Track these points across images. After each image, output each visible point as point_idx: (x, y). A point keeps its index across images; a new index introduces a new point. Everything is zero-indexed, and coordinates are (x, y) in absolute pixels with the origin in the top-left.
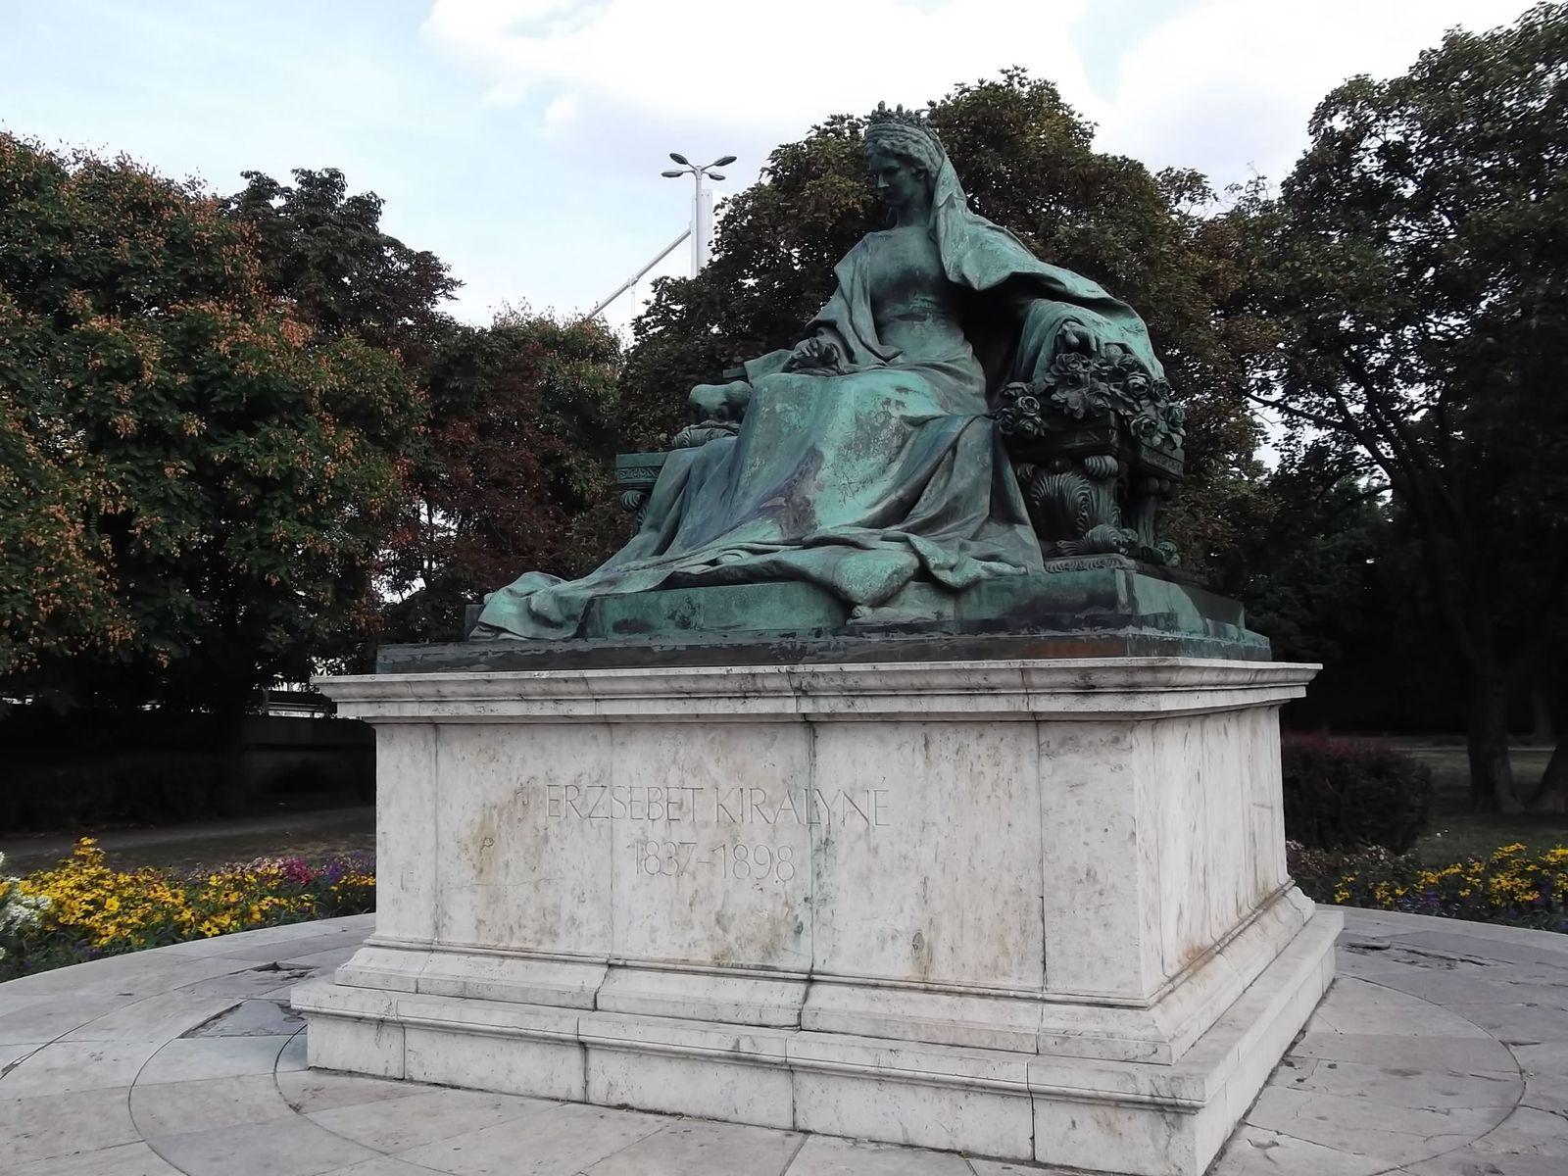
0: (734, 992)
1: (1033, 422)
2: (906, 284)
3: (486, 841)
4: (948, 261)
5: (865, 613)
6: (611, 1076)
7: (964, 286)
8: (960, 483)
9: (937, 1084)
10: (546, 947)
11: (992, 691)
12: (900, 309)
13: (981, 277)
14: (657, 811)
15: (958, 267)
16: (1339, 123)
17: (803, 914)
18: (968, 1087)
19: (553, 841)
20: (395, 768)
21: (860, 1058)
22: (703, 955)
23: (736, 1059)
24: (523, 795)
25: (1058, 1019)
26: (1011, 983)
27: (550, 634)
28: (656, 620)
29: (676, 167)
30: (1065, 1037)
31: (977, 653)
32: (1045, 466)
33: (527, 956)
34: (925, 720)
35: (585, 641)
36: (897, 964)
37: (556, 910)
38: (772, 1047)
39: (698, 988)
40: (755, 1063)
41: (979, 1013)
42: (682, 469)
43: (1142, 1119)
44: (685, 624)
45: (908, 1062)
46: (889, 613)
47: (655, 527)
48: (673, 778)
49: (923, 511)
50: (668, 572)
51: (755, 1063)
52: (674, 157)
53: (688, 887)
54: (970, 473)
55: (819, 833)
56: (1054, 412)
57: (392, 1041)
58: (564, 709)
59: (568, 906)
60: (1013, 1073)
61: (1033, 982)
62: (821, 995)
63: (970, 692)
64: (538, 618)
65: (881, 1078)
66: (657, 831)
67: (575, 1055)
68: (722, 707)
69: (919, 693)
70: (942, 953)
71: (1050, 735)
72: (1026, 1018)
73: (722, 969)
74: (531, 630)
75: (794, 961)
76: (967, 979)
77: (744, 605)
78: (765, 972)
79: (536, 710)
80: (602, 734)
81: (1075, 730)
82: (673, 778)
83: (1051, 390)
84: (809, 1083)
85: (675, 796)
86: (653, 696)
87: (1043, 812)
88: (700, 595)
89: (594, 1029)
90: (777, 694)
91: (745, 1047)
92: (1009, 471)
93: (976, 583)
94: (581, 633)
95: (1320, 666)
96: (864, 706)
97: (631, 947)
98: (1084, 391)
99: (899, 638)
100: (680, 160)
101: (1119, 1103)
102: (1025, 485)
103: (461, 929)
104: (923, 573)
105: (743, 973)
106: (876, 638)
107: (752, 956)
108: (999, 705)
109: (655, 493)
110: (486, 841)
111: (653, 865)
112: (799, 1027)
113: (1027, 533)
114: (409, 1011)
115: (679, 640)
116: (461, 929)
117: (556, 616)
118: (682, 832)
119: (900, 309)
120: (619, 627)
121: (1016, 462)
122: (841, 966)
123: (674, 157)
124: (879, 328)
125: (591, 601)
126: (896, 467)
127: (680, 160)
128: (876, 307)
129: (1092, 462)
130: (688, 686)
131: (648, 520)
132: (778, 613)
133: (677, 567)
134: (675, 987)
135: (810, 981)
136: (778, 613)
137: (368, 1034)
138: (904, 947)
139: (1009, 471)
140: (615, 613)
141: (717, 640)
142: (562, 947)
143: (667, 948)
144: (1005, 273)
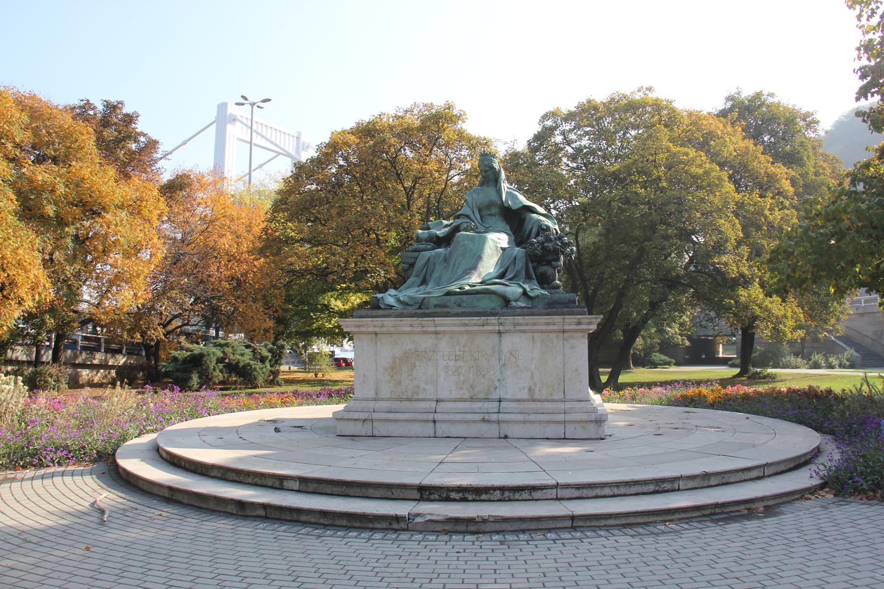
0: (477, 405)
1: (539, 252)
2: (491, 205)
6: (442, 429)
9: (540, 422)
10: (415, 397)
11: (554, 324)
12: (488, 212)
14: (452, 357)
16: (549, 123)
17: (497, 384)
18: (548, 422)
19: (417, 367)
21: (520, 417)
22: (467, 396)
23: (484, 420)
25: (568, 405)
26: (555, 397)
28: (448, 304)
29: (243, 101)
30: (572, 408)
31: (547, 314)
33: (409, 400)
34: (533, 332)
35: (421, 309)
36: (524, 395)
37: (418, 387)
38: (494, 417)
39: (467, 405)
40: (489, 421)
41: (548, 405)
42: (427, 258)
43: (592, 425)
44: (459, 305)
45: (533, 417)
47: (417, 276)
48: (457, 349)
49: (509, 275)
51: (489, 421)
52: (242, 97)
53: (462, 378)
54: (520, 265)
55: (502, 362)
56: (544, 248)
57: (368, 426)
58: (425, 329)
59: (422, 385)
60: (561, 417)
61: (561, 396)
62: (503, 404)
63: (548, 324)
65: (524, 422)
66: (452, 363)
67: (432, 424)
68: (476, 328)
69: (534, 324)
70: (537, 392)
71: (566, 335)
72: (561, 406)
73: (472, 399)
75: (496, 396)
76: (544, 397)
77: (478, 300)
78: (487, 400)
79: (415, 329)
80: (434, 336)
81: (573, 334)
82: (457, 349)
83: (543, 243)
84: (503, 426)
85: (458, 353)
86: (455, 325)
87: (564, 355)
88: (465, 297)
89: (438, 417)
90: (494, 324)
91: (487, 417)
92: (530, 265)
93: (538, 296)
94: (420, 308)
96: (518, 328)
97: (444, 395)
99: (525, 310)
100: (246, 99)
101: (587, 422)
102: (534, 269)
103: (385, 392)
104: (525, 293)
105: (480, 400)
107: (482, 396)
108: (556, 327)
109: (416, 265)
111: (450, 373)
112: (499, 413)
113: (535, 282)
114: (375, 416)
115: (460, 310)
118: (459, 363)
119: (488, 212)
120: (435, 306)
121: (532, 262)
122: (508, 396)
123: (242, 97)
125: (424, 298)
127: (246, 99)
128: (480, 210)
130: (467, 322)
131: (414, 273)
134: (460, 405)
135: (500, 401)
136: (486, 303)
137: (360, 424)
138: (526, 390)
139: (530, 265)
140: (434, 302)
141: (471, 310)
142: (421, 396)
143: (455, 395)
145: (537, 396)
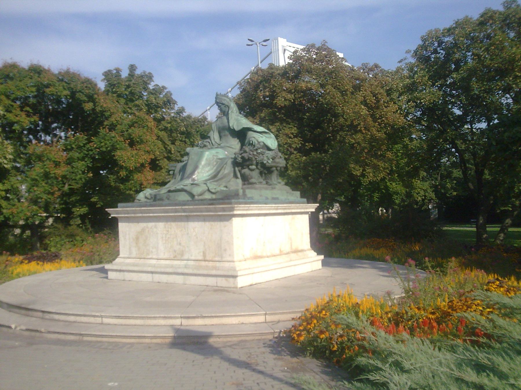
3: (137, 238)
4: (231, 125)
5: (196, 197)
7: (234, 130)
8: (226, 172)
13: (237, 128)
15: (233, 126)
20: (122, 227)
24: (143, 230)
27: (148, 201)
29: (250, 43)
32: (243, 168)
36: (200, 258)
46: (201, 197)
50: (168, 190)
64: (146, 198)
74: (146, 200)
76: (210, 259)
95: (318, 205)
98: (248, 154)
100: (252, 41)
102: (240, 171)
104: (209, 190)
106: (197, 202)
110: (137, 238)
116: (134, 255)
117: (149, 197)
124: (221, 137)
126: (215, 168)
127: (252, 41)
128: (219, 133)
129: (250, 167)
132: (183, 197)
133: (170, 189)
138: (202, 254)
139: (236, 168)
144: (241, 127)
145: (208, 258)
